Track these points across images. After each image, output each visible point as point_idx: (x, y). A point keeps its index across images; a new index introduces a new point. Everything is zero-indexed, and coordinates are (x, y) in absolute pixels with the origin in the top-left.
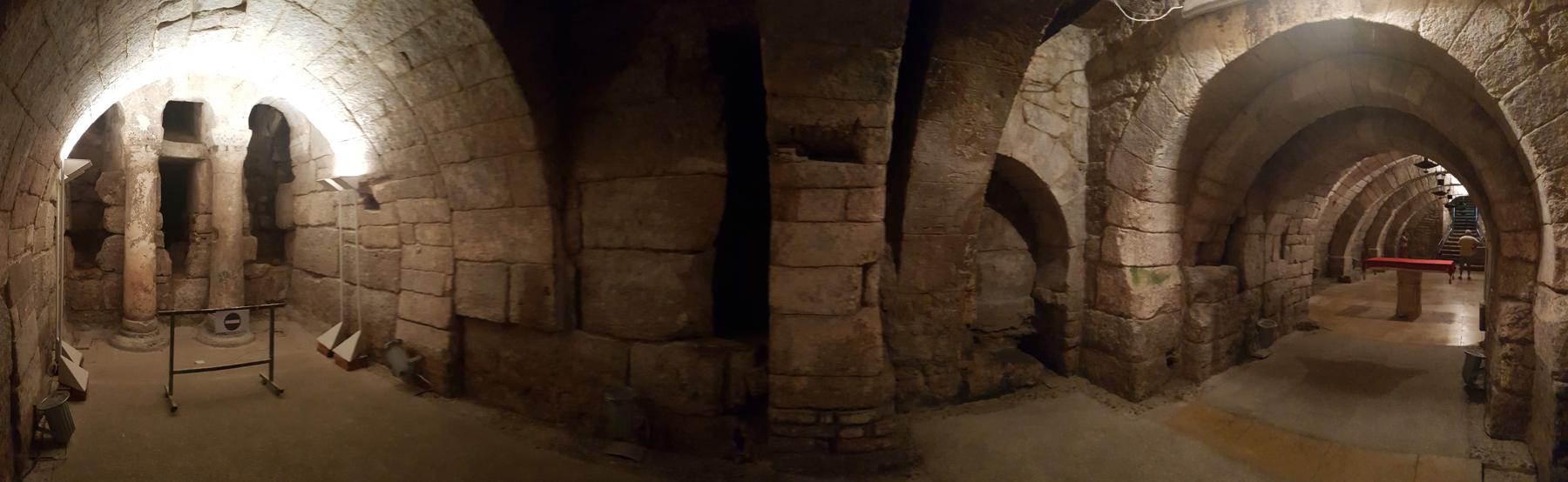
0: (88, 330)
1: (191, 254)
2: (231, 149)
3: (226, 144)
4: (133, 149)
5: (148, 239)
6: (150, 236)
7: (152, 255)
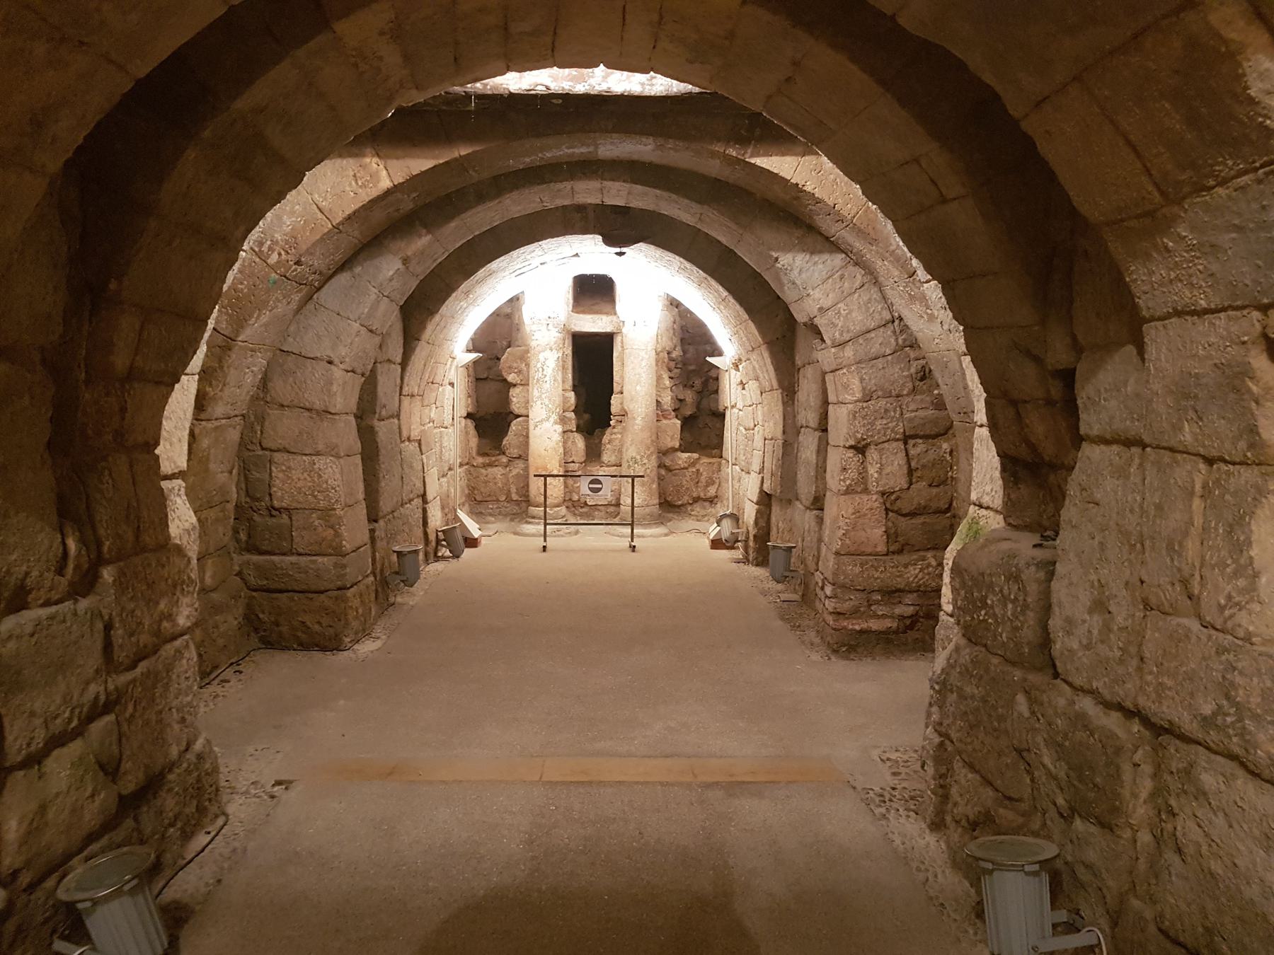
0: (493, 523)
1: (605, 439)
4: (534, 328)
5: (552, 420)
6: (554, 417)
7: (557, 437)
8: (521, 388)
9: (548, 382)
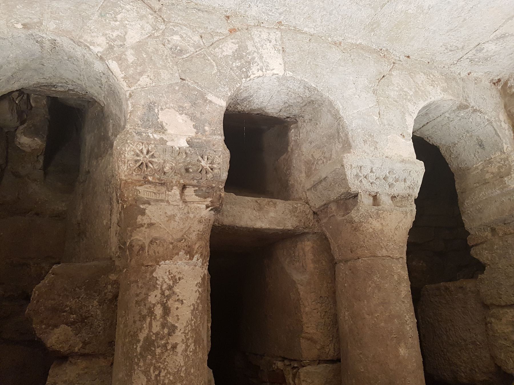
2: (385, 200)
3: (375, 189)
8: (82, 364)
9: (180, 348)
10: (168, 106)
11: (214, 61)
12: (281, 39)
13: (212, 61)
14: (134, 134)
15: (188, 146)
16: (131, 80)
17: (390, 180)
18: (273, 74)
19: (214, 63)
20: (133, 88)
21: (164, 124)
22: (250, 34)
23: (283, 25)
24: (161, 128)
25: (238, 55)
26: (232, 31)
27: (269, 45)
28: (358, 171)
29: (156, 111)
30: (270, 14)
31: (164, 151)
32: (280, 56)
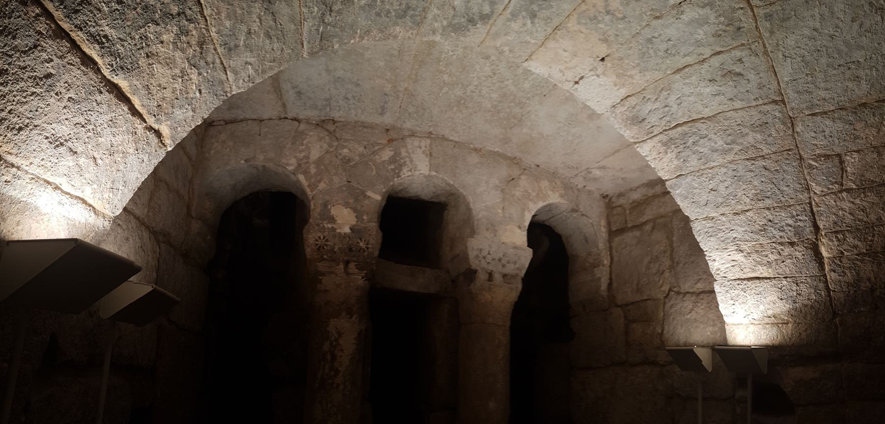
2: (498, 277)
3: (490, 268)
10: (338, 203)
11: (374, 165)
12: (431, 145)
13: (372, 165)
14: (315, 226)
15: (350, 232)
16: (313, 186)
17: (503, 262)
18: (421, 174)
19: (374, 167)
20: (314, 193)
21: (335, 217)
22: (404, 143)
23: (433, 134)
24: (332, 220)
25: (393, 160)
26: (390, 141)
27: (419, 151)
28: (478, 253)
29: (329, 207)
30: (422, 126)
31: (334, 236)
32: (427, 159)
